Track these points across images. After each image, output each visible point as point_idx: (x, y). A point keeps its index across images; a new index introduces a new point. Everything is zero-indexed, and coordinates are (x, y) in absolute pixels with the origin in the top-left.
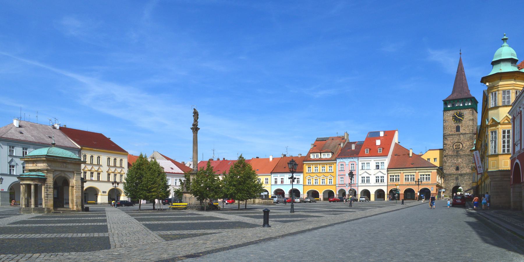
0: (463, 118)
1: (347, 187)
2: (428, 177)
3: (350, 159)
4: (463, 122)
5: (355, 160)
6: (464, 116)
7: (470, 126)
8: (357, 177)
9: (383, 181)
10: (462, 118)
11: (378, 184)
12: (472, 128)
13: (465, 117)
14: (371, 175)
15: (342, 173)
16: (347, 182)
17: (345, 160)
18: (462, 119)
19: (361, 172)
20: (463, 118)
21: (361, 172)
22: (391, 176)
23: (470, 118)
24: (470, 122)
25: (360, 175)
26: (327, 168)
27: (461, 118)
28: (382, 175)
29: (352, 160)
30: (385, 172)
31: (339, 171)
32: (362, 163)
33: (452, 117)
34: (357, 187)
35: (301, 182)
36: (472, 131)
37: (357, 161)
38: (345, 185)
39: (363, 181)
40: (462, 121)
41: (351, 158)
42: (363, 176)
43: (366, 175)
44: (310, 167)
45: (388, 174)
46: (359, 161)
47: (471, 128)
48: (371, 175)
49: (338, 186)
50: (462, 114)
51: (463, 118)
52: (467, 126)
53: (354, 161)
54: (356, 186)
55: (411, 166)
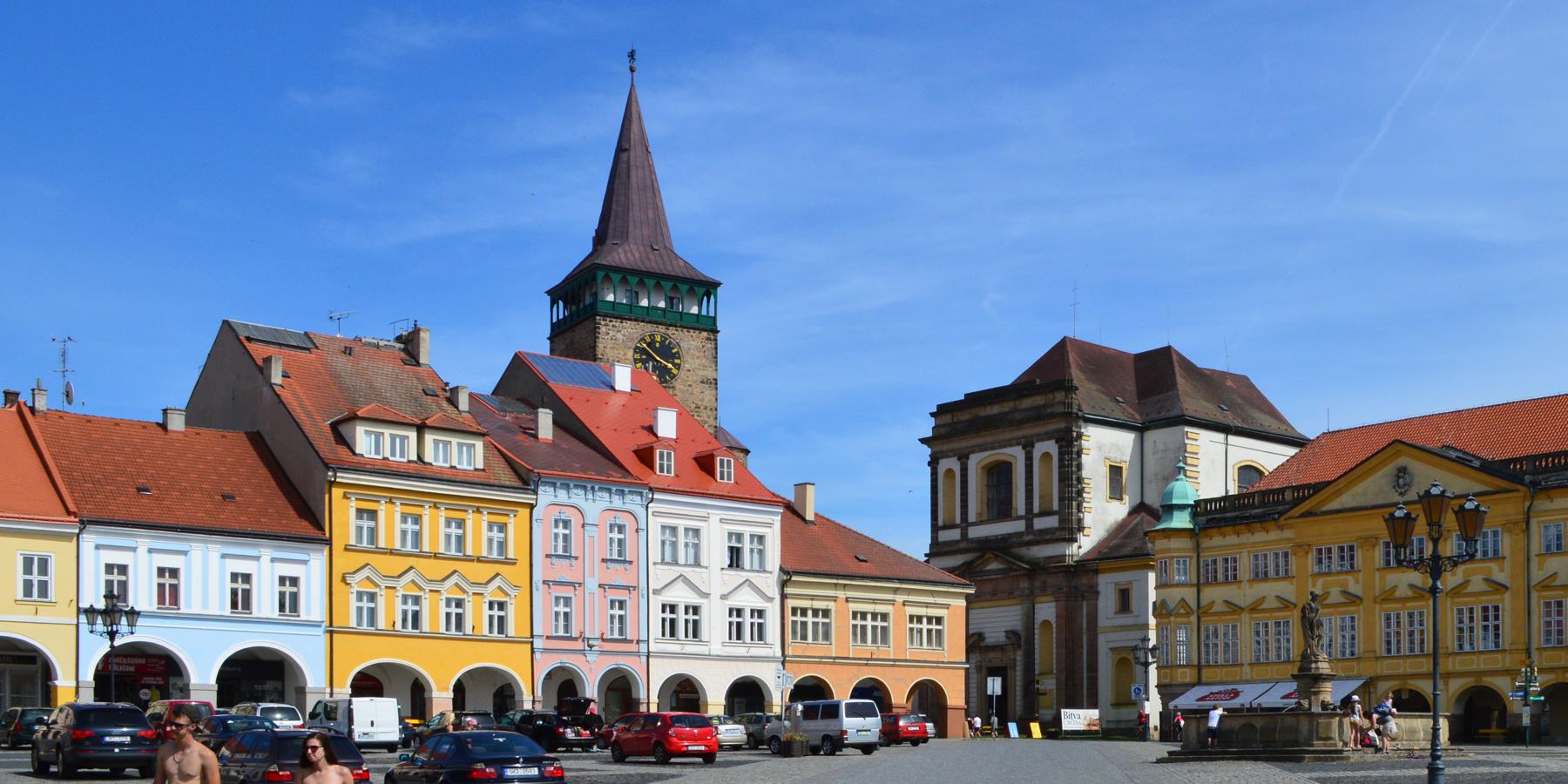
0: (678, 367)
1: (591, 657)
2: (936, 630)
3: (606, 495)
4: (678, 384)
5: (633, 503)
6: (679, 358)
7: (706, 408)
8: (643, 602)
9: (761, 637)
10: (674, 364)
11: (740, 650)
12: (711, 421)
13: (687, 366)
14: (706, 595)
15: (563, 571)
16: (593, 631)
17: (578, 497)
18: (675, 371)
19: (660, 575)
20: (679, 365)
21: (660, 575)
22: (794, 611)
23: (705, 373)
24: (707, 392)
25: (656, 592)
26: (479, 532)
27: (670, 366)
28: (759, 604)
29: (617, 502)
30: (770, 583)
31: (548, 556)
32: (664, 528)
33: (631, 352)
34: (644, 659)
35: (313, 605)
36: (712, 431)
37: (640, 512)
38: (579, 645)
39: (671, 628)
40: (672, 378)
41: (614, 489)
42: (670, 597)
43: (681, 596)
44: (373, 514)
45: (784, 597)
46: (650, 511)
47: (709, 417)
48: (706, 595)
49: (546, 650)
50: (670, 347)
51: (679, 365)
52: (693, 406)
53: (628, 507)
54: (638, 654)
55: (854, 568)
